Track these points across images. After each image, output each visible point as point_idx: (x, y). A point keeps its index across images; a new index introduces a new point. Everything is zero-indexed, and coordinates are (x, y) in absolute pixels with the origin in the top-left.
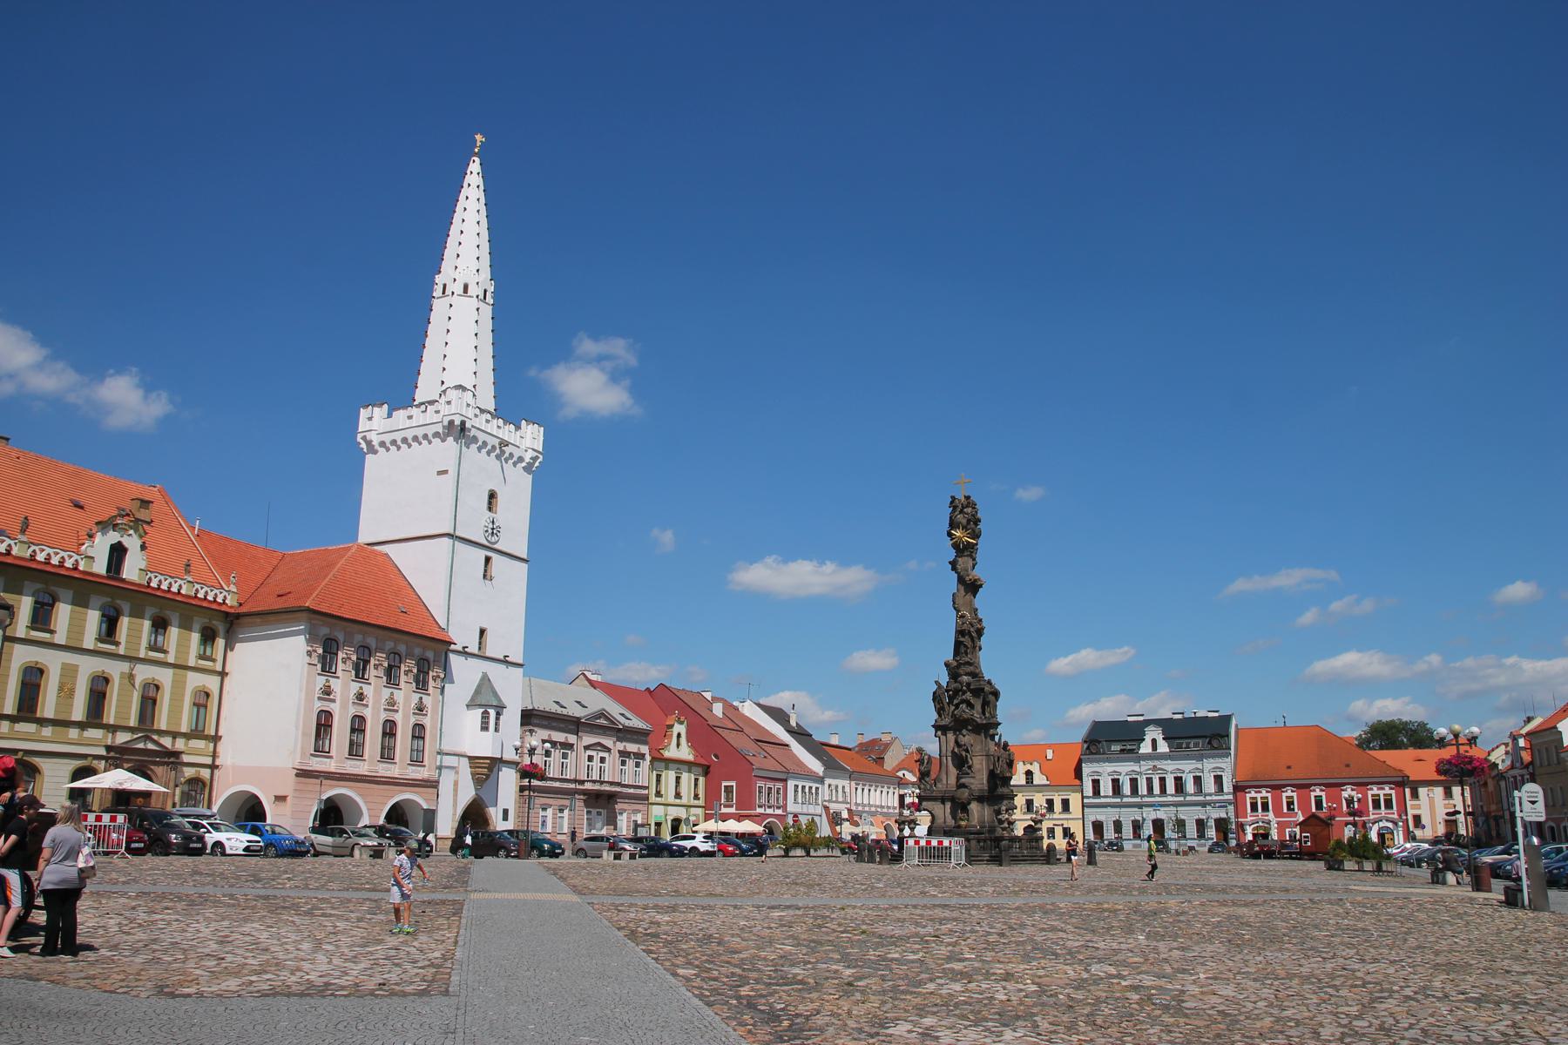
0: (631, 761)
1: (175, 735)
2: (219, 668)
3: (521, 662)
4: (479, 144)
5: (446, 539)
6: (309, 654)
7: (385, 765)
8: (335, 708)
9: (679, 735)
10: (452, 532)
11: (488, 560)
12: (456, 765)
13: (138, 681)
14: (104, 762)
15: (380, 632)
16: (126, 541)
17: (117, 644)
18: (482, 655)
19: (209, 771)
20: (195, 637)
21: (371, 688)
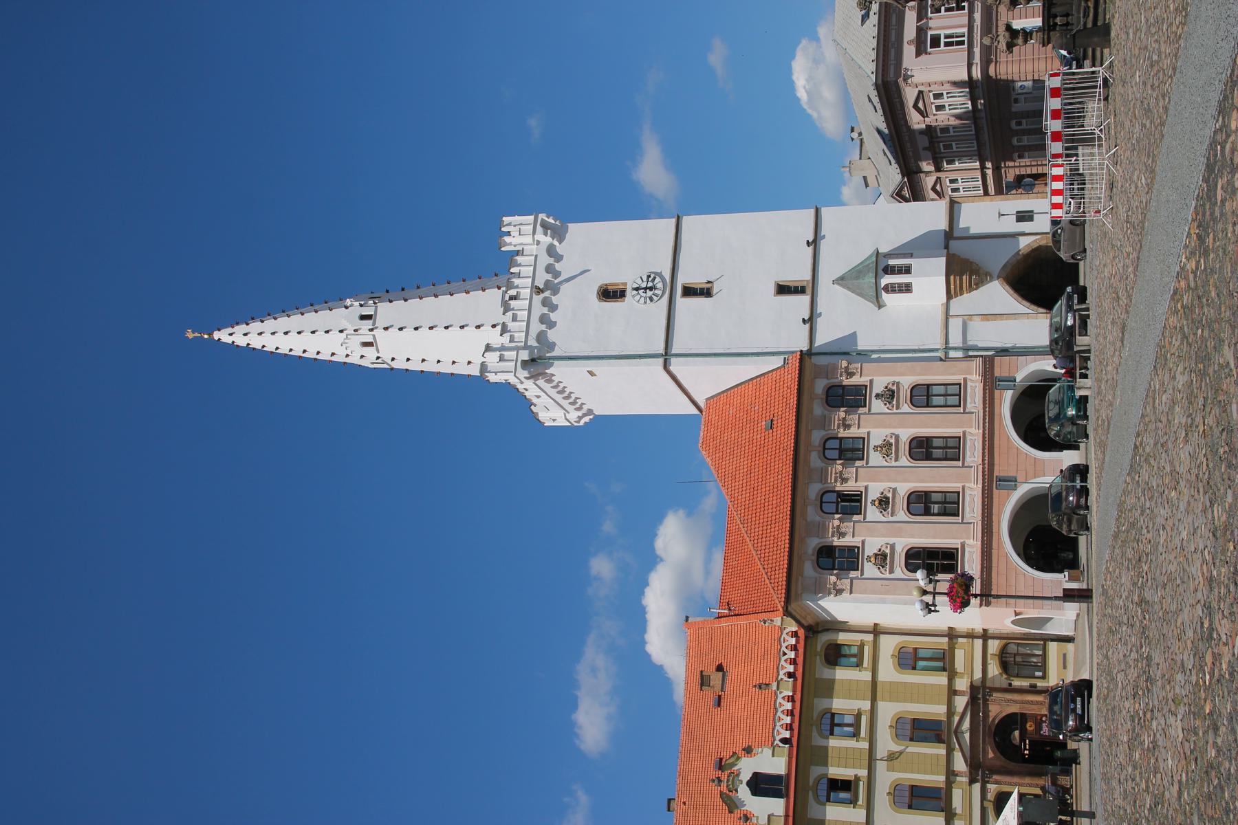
0: (932, 23)
1: (952, 692)
2: (870, 637)
3: (812, 211)
4: (197, 335)
5: (672, 368)
6: (839, 592)
7: (967, 509)
8: (903, 544)
10: (661, 360)
11: (689, 292)
12: (960, 320)
13: (895, 748)
14: (989, 786)
15: (805, 397)
16: (746, 776)
17: (861, 646)
18: (811, 285)
19: (990, 642)
20: (842, 674)
21: (871, 485)
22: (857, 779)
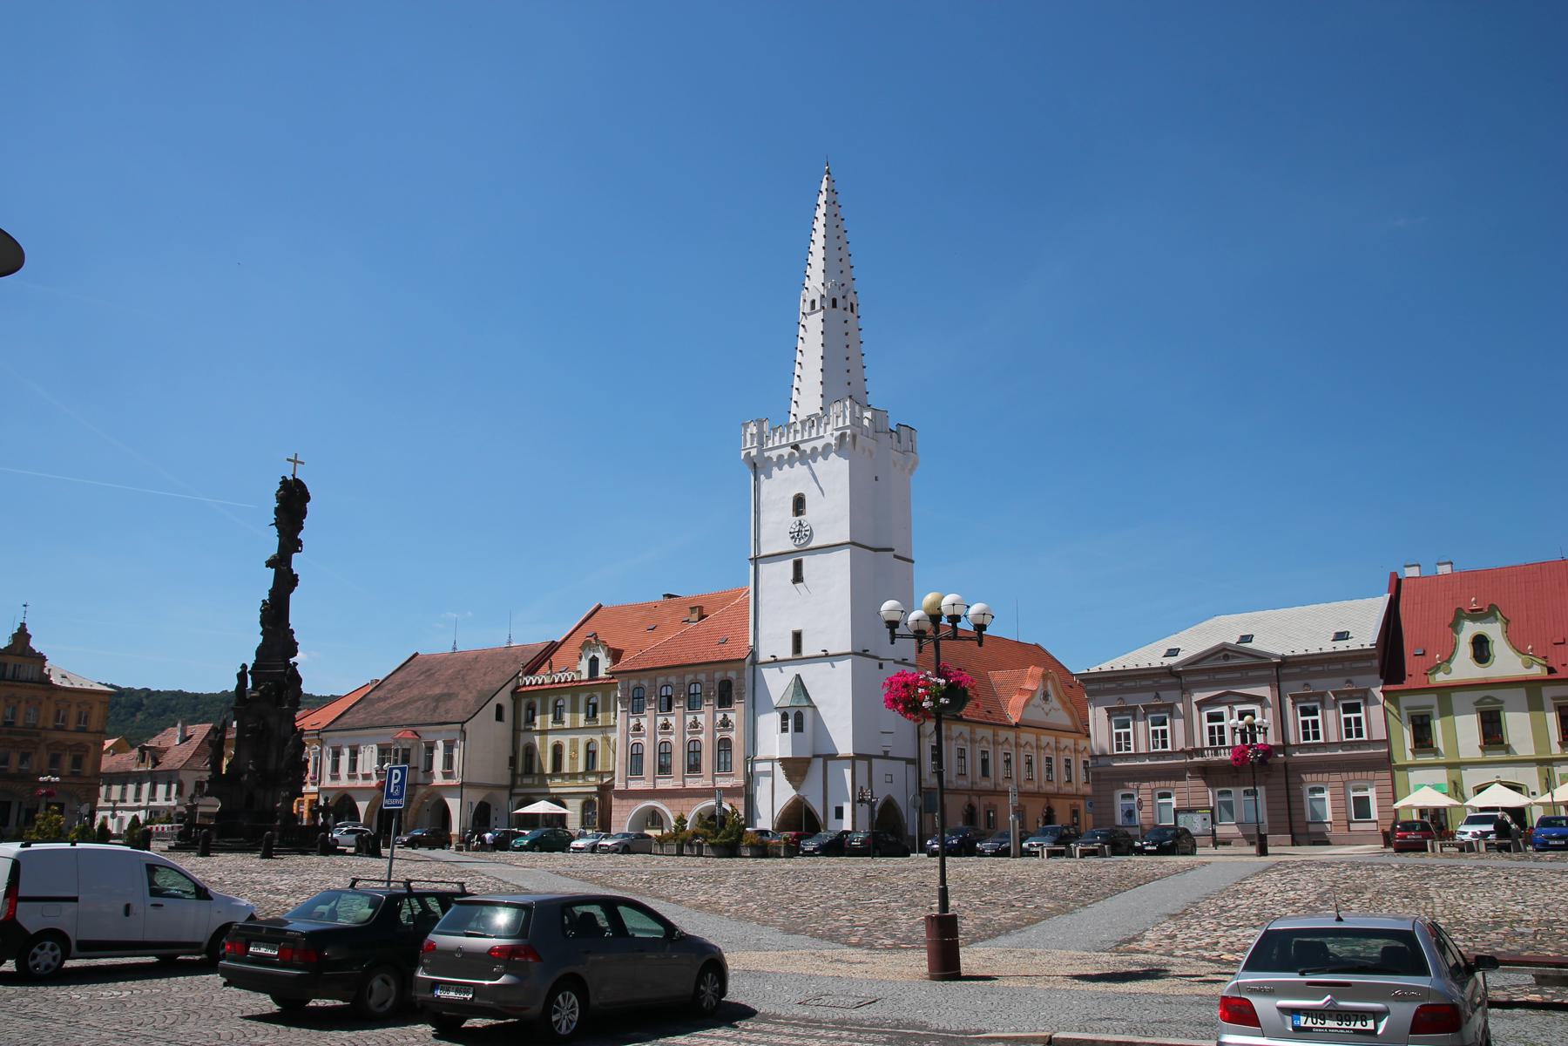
11: (798, 566)
16: (597, 655)
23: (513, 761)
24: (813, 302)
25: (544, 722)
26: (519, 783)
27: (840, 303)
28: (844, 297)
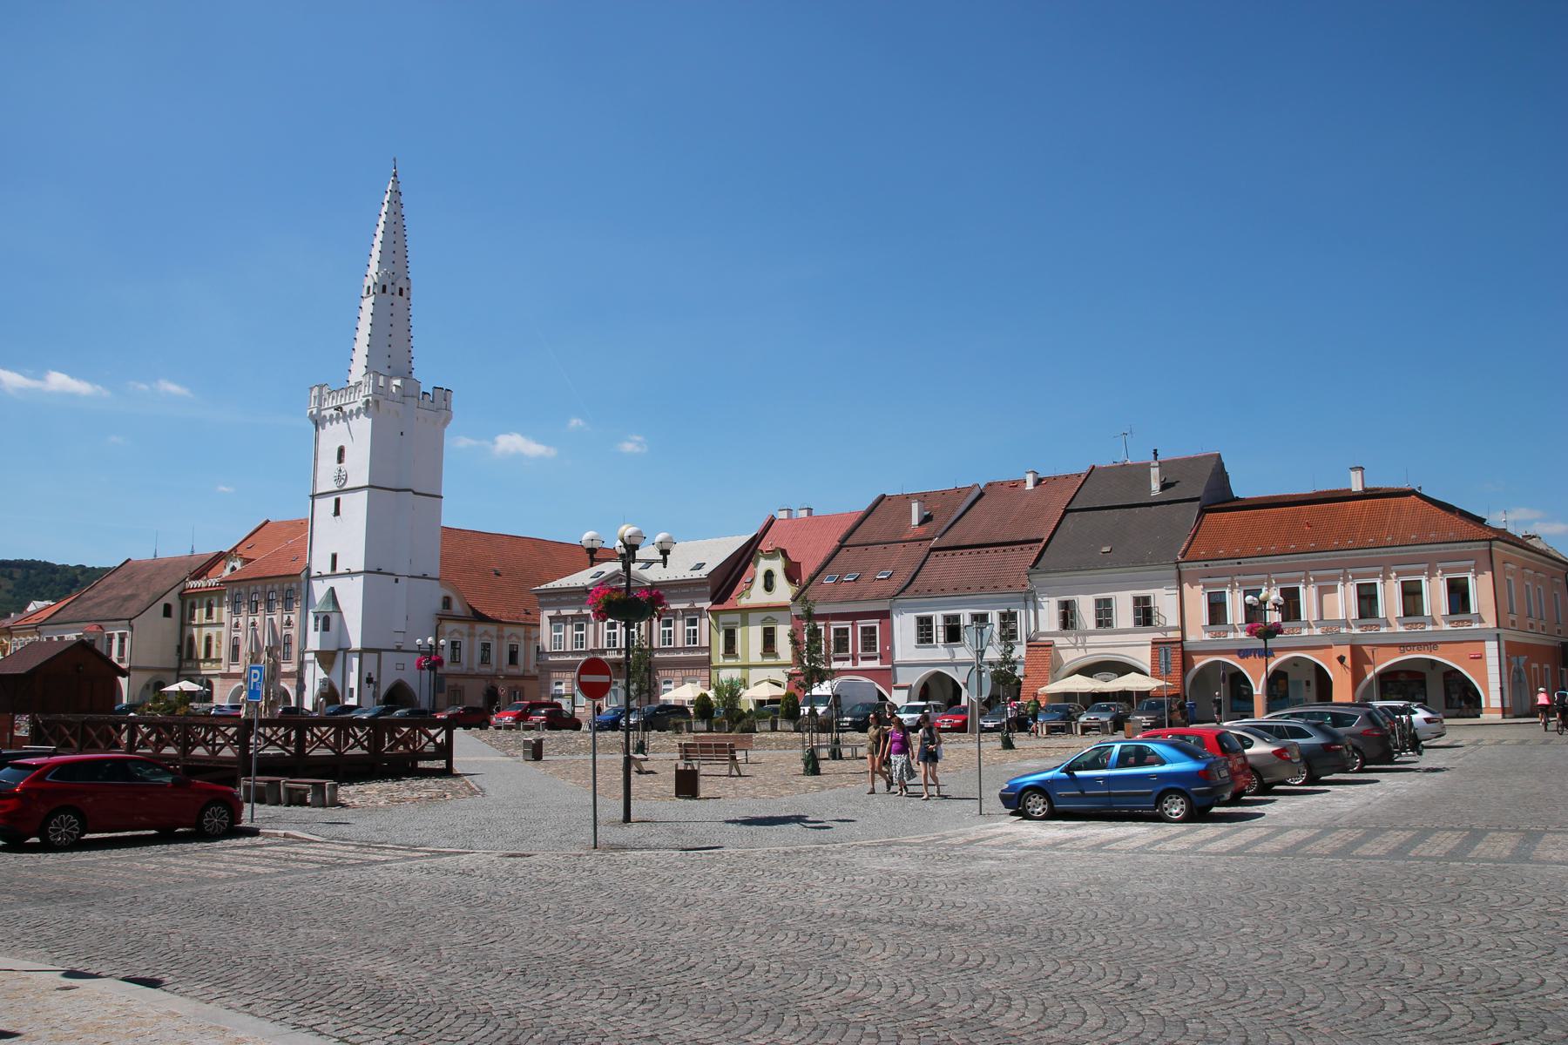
9: (769, 575)
11: (337, 501)
22: (212, 618)
23: (180, 649)
24: (369, 287)
25: (200, 618)
26: (184, 666)
27: (388, 289)
28: (393, 284)
